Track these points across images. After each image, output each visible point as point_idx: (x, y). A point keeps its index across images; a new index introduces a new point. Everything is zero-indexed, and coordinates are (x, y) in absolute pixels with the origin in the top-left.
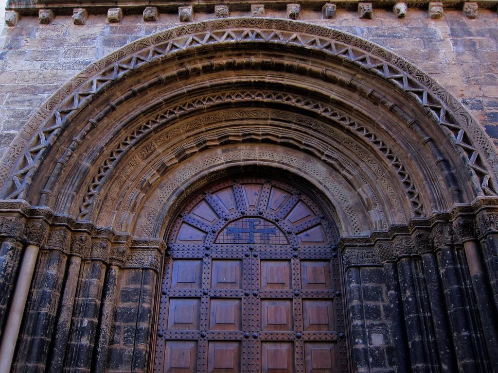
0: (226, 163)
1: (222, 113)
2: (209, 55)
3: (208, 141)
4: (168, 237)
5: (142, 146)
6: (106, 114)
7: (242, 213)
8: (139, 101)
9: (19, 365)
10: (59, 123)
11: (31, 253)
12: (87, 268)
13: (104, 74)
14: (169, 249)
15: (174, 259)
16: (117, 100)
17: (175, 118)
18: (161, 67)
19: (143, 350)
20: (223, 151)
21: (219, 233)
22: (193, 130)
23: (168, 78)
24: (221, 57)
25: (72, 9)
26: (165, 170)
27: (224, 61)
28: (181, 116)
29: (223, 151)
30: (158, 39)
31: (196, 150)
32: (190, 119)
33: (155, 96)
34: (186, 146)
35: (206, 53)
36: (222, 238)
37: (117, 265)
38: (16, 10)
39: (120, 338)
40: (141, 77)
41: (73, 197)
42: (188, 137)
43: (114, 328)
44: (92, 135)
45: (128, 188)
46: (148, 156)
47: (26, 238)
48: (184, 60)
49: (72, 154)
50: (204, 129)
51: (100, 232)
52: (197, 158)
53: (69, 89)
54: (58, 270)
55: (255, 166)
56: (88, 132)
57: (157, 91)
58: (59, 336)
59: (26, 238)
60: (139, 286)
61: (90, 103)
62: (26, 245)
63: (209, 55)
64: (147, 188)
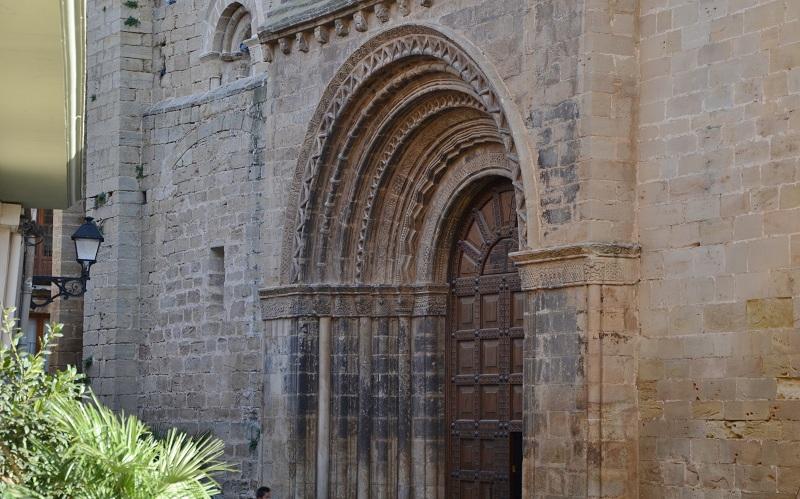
0: (470, 176)
1: (440, 124)
2: (387, 74)
3: (449, 153)
4: (450, 277)
5: (392, 181)
6: (341, 168)
7: (499, 234)
8: (363, 141)
9: (335, 418)
10: (307, 193)
11: (324, 323)
12: (376, 324)
13: (323, 128)
14: (453, 286)
15: (459, 297)
16: (343, 150)
17: (400, 147)
18: (360, 102)
19: (431, 398)
20: (467, 160)
21: (485, 261)
22: (429, 145)
23: (368, 112)
24: (397, 73)
25: (295, 34)
26: (426, 198)
27: (399, 78)
28: (405, 140)
29: (467, 160)
30: (341, 76)
31: (444, 166)
32: (419, 137)
33: (373, 130)
34: (431, 164)
35: (384, 73)
36: (489, 267)
37: (406, 316)
38: (266, 43)
39: (416, 386)
40: (350, 118)
41: (342, 263)
42: (429, 155)
43: (411, 380)
44: (342, 191)
45: (397, 231)
46: (403, 189)
47: (314, 312)
48: (374, 86)
49: (329, 220)
50: (437, 142)
51: (374, 289)
52: (450, 174)
53: (305, 154)
54: (347, 334)
55: (489, 177)
56: (334, 192)
57: (373, 123)
58: (361, 392)
59: (314, 312)
60: (423, 334)
61: (324, 163)
62: (318, 318)
63: (387, 74)
64: (418, 223)
